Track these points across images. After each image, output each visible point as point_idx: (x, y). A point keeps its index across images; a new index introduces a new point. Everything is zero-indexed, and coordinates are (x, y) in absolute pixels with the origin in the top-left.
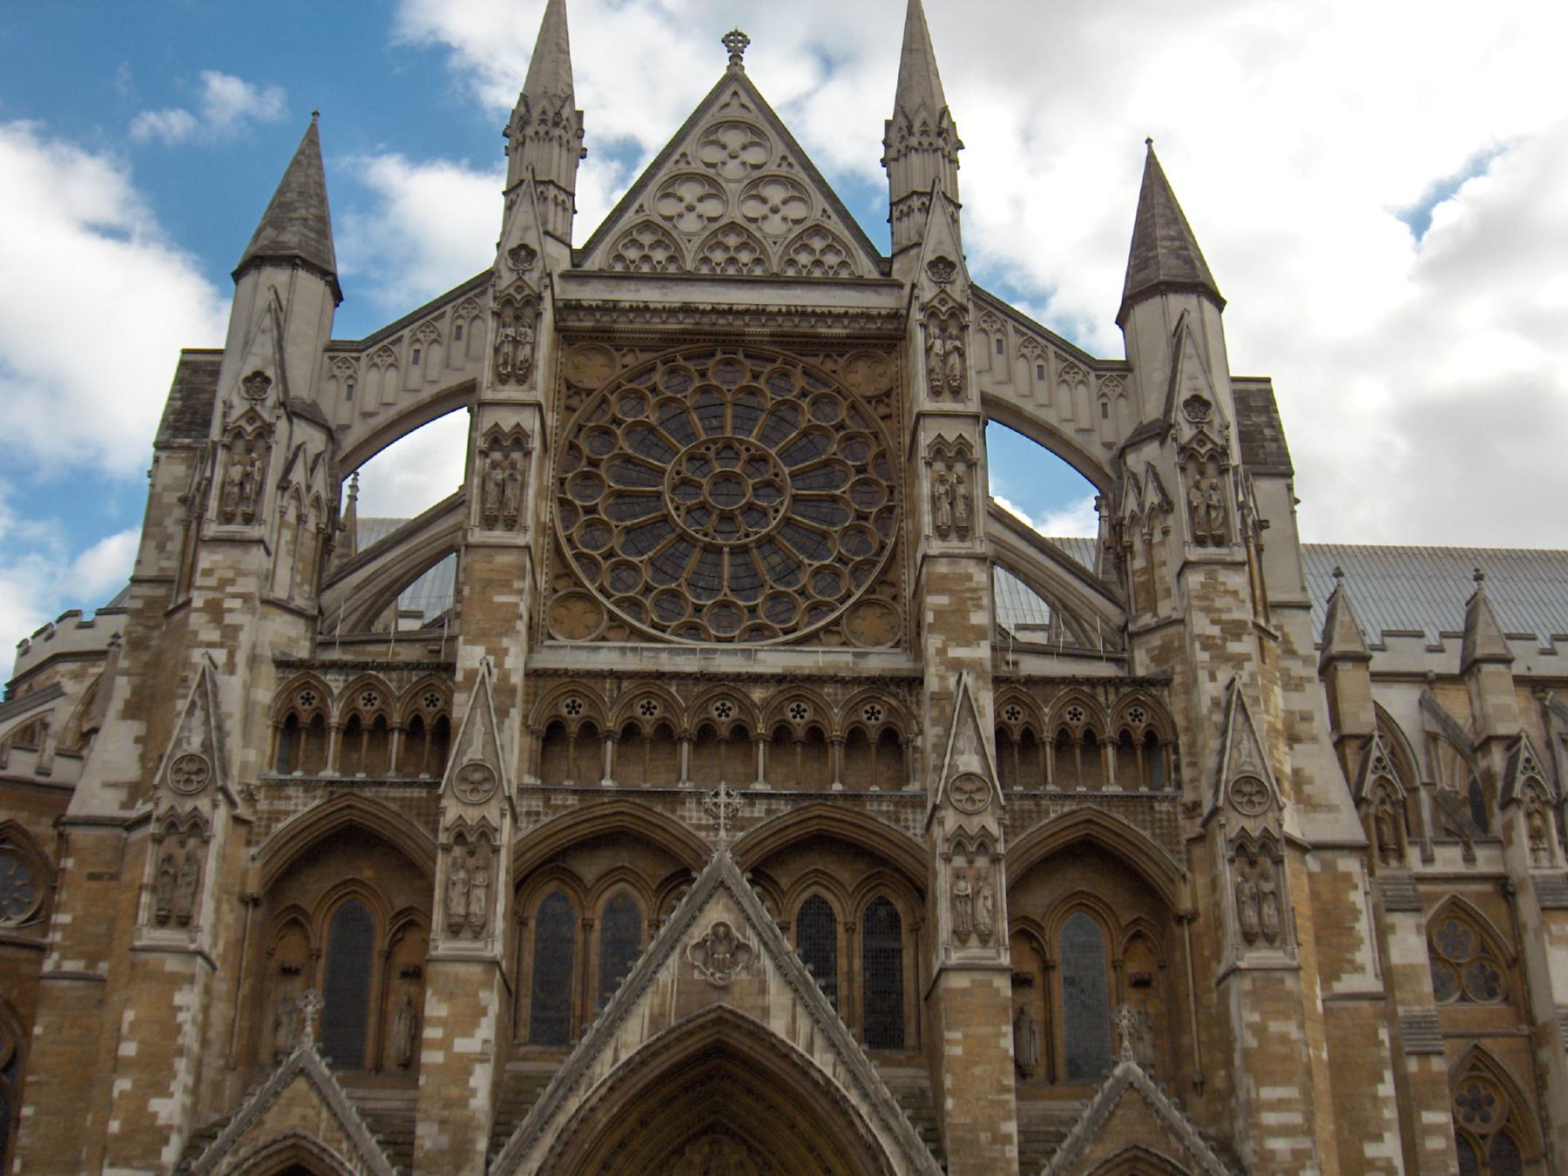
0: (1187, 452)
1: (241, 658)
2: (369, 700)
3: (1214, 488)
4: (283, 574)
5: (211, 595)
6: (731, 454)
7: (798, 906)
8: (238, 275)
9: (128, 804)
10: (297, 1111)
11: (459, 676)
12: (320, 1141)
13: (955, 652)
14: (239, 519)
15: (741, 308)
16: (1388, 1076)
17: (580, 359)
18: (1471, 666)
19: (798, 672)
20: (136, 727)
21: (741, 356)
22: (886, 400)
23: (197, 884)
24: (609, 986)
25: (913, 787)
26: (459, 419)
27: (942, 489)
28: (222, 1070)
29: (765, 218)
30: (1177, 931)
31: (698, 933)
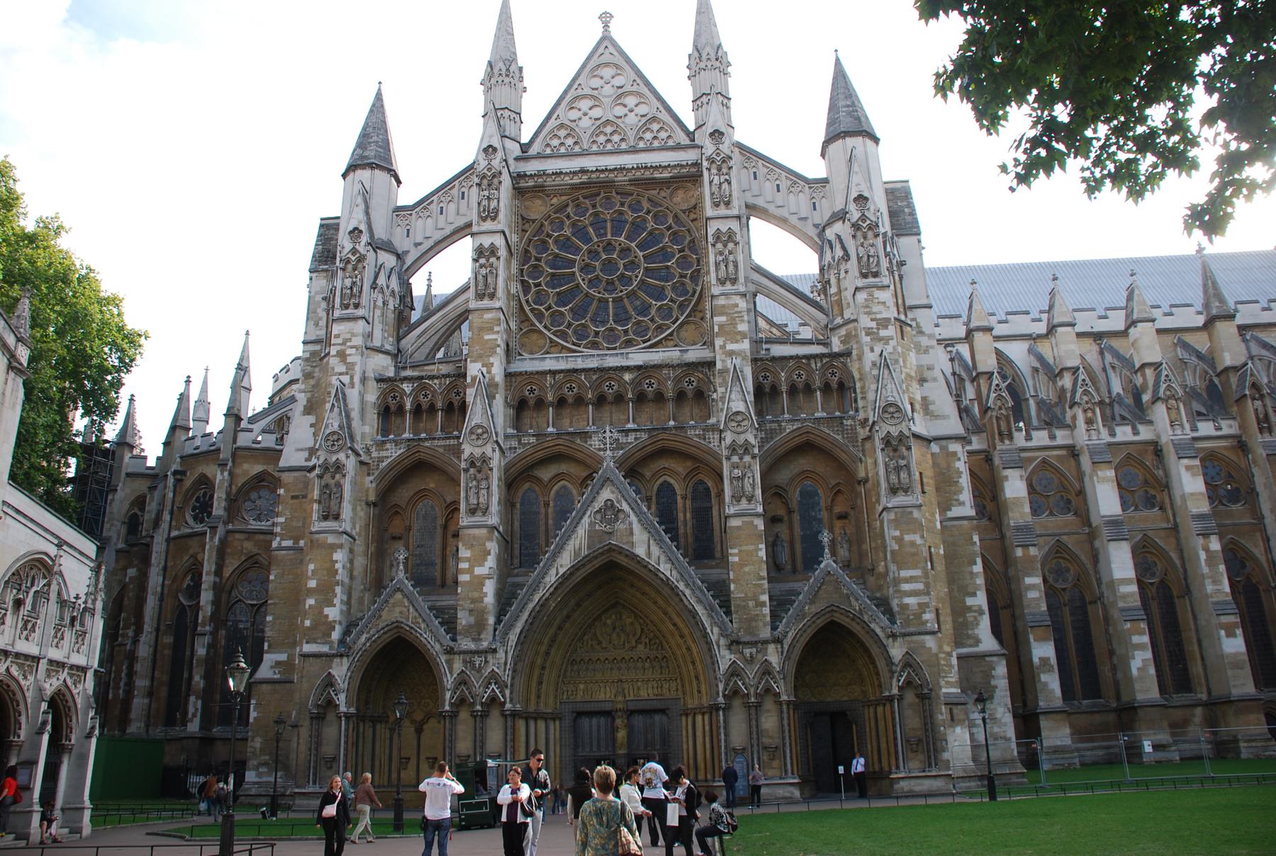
0: (856, 226)
1: (357, 379)
2: (426, 396)
3: (872, 245)
4: (378, 334)
5: (339, 348)
6: (611, 247)
7: (655, 488)
8: (344, 176)
9: (308, 460)
10: (398, 609)
11: (469, 380)
12: (410, 623)
13: (730, 347)
14: (352, 306)
15: (612, 167)
16: (979, 560)
17: (527, 203)
18: (1052, 329)
19: (652, 363)
20: (311, 419)
21: (614, 194)
26: (468, 241)
27: (721, 258)
28: (362, 591)
29: (626, 115)
30: (858, 488)
31: (598, 505)
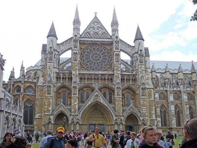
2: (64, 76)
18: (165, 72)
23: (51, 91)
24: (87, 99)
25: (113, 83)
31: (95, 95)
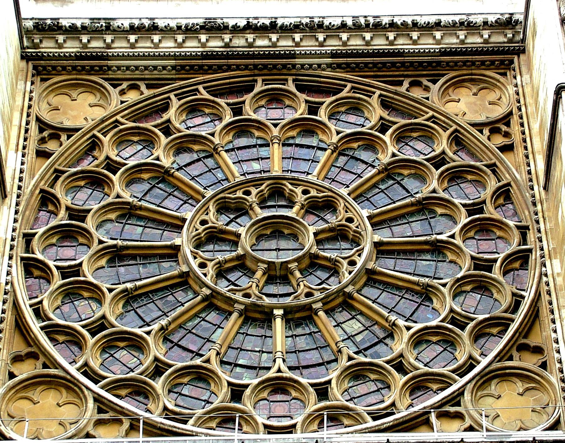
15: (287, 22)
17: (56, 100)
21: (291, 87)
22: (504, 128)
